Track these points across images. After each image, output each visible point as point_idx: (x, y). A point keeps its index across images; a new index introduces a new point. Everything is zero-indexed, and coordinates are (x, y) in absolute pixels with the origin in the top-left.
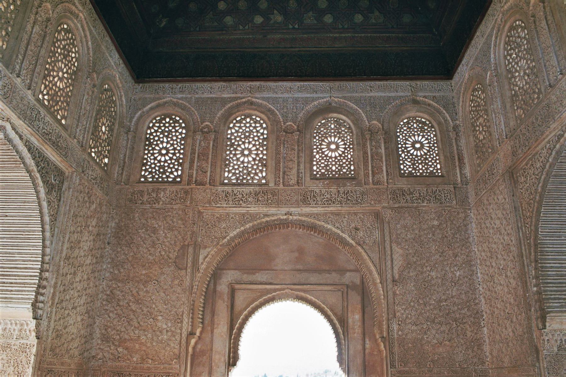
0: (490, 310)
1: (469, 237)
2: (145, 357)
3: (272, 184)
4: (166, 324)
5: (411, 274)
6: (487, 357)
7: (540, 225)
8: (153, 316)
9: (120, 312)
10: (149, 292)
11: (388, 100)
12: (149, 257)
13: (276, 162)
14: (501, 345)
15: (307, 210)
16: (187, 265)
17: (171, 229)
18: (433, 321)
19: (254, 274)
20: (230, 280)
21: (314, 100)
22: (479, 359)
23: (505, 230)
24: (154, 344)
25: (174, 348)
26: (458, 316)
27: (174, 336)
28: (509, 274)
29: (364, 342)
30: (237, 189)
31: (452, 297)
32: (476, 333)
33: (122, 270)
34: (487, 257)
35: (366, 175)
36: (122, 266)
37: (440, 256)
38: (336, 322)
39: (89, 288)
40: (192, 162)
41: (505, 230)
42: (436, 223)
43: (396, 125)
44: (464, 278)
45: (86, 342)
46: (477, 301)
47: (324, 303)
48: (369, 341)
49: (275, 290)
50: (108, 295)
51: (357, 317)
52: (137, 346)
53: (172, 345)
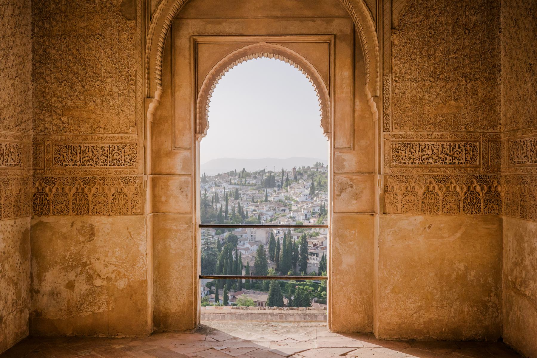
2: (95, 126)
4: (117, 87)
5: (415, 20)
6: (500, 119)
8: (100, 78)
9: (58, 75)
10: (92, 50)
12: (88, 5)
14: (517, 103)
16: (136, 14)
18: (438, 77)
19: (220, 23)
20: (191, 31)
24: (105, 111)
25: (130, 114)
27: (128, 101)
29: (354, 103)
31: (464, 48)
32: (489, 92)
33: (54, 24)
36: (54, 19)
38: (320, 80)
39: (17, 45)
44: (481, 24)
45: (21, 112)
46: (495, 53)
47: (306, 58)
48: (360, 101)
49: (247, 43)
50: (40, 56)
52: (85, 114)
53: (127, 111)
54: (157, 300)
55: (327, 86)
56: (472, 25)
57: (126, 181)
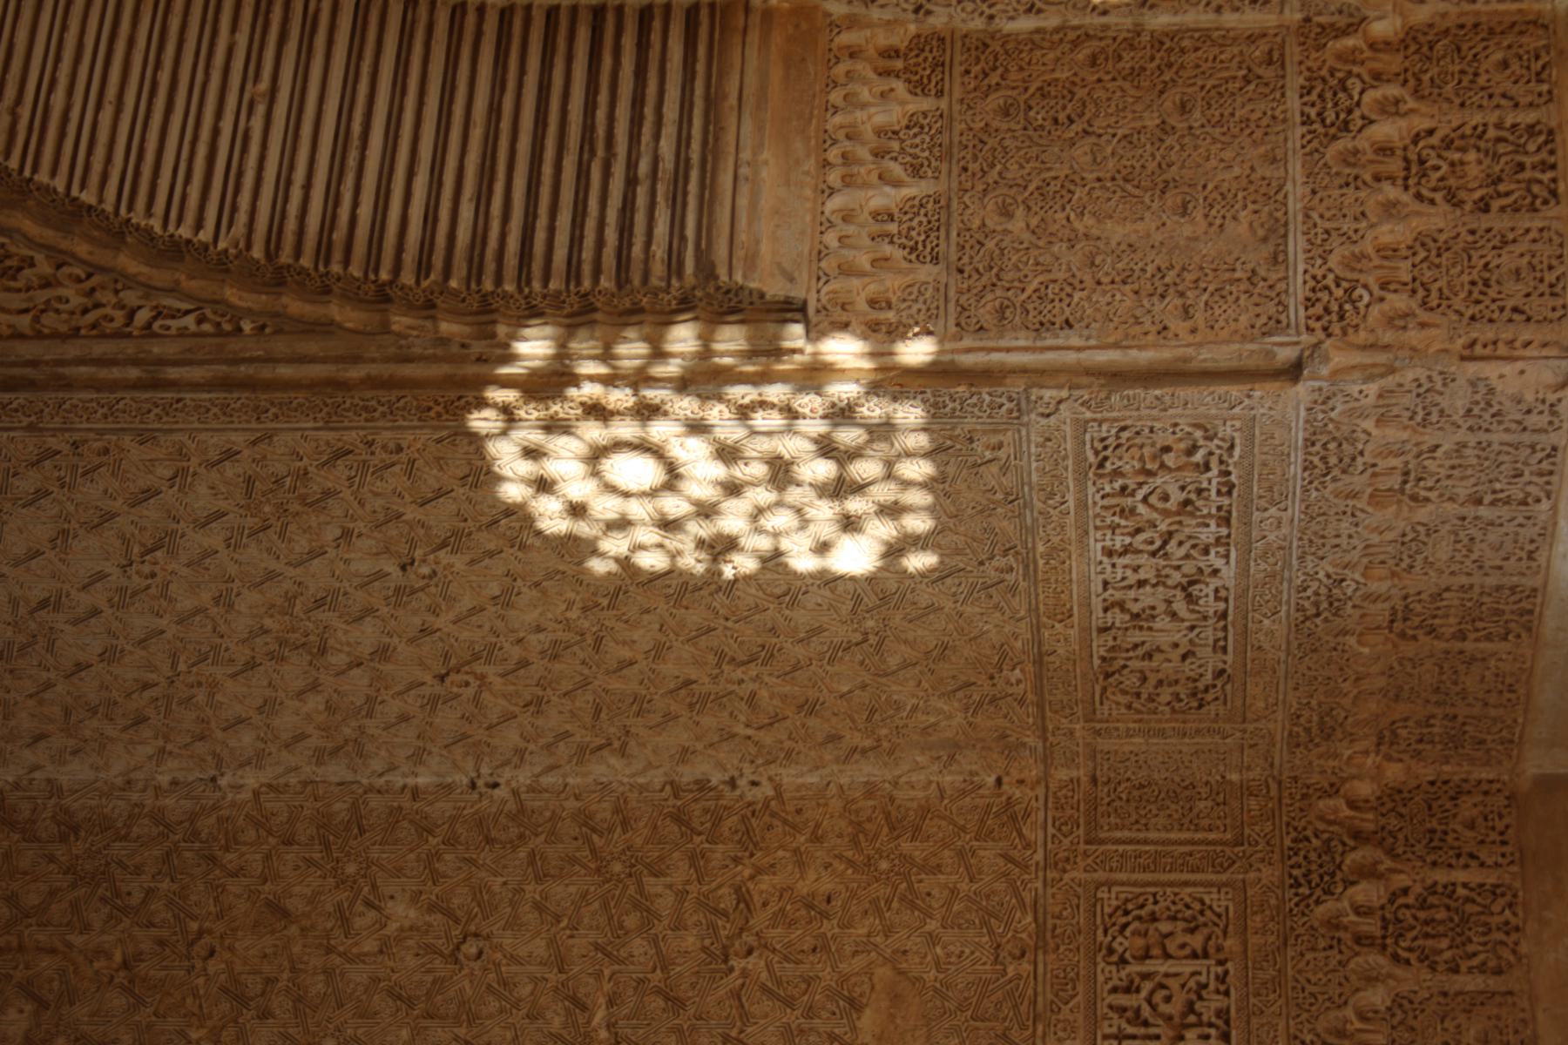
0: (669, 717)
1: (158, 817)
7: (156, 224)
22: (983, 834)
23: (150, 493)
26: (690, 941)
28: (441, 517)
34: (314, 687)
37: (265, 1015)
41: (150, 493)
44: (436, 877)
46: (603, 811)
56: (437, 919)
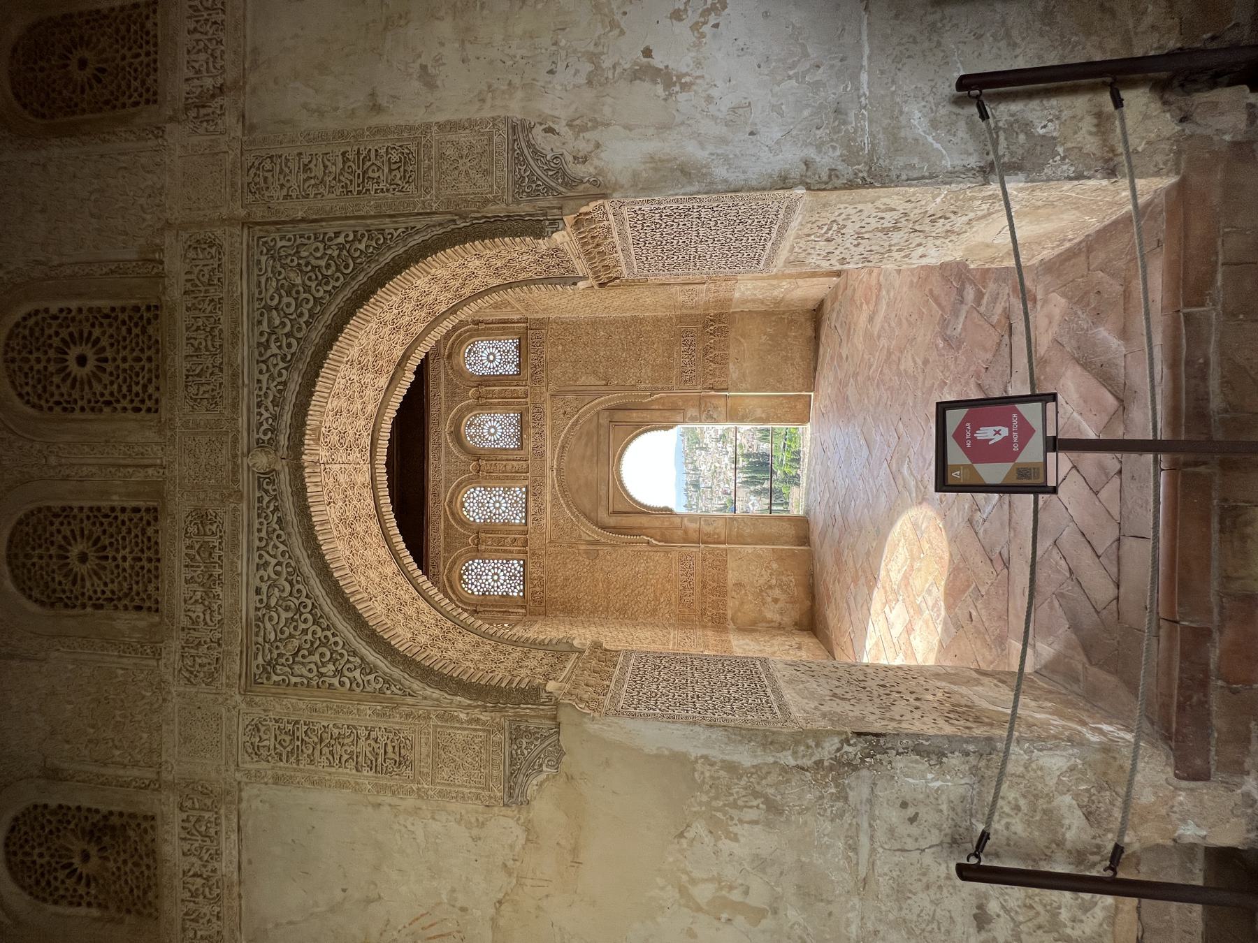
3: (527, 483)
11: (449, 381)
13: (508, 478)
15: (549, 453)
17: (565, 564)
21: (447, 446)
30: (531, 512)
35: (519, 404)
40: (505, 551)
42: (560, 348)
43: (472, 375)
51: (634, 414)
54: (786, 543)
55: (641, 428)
57: (704, 560)
